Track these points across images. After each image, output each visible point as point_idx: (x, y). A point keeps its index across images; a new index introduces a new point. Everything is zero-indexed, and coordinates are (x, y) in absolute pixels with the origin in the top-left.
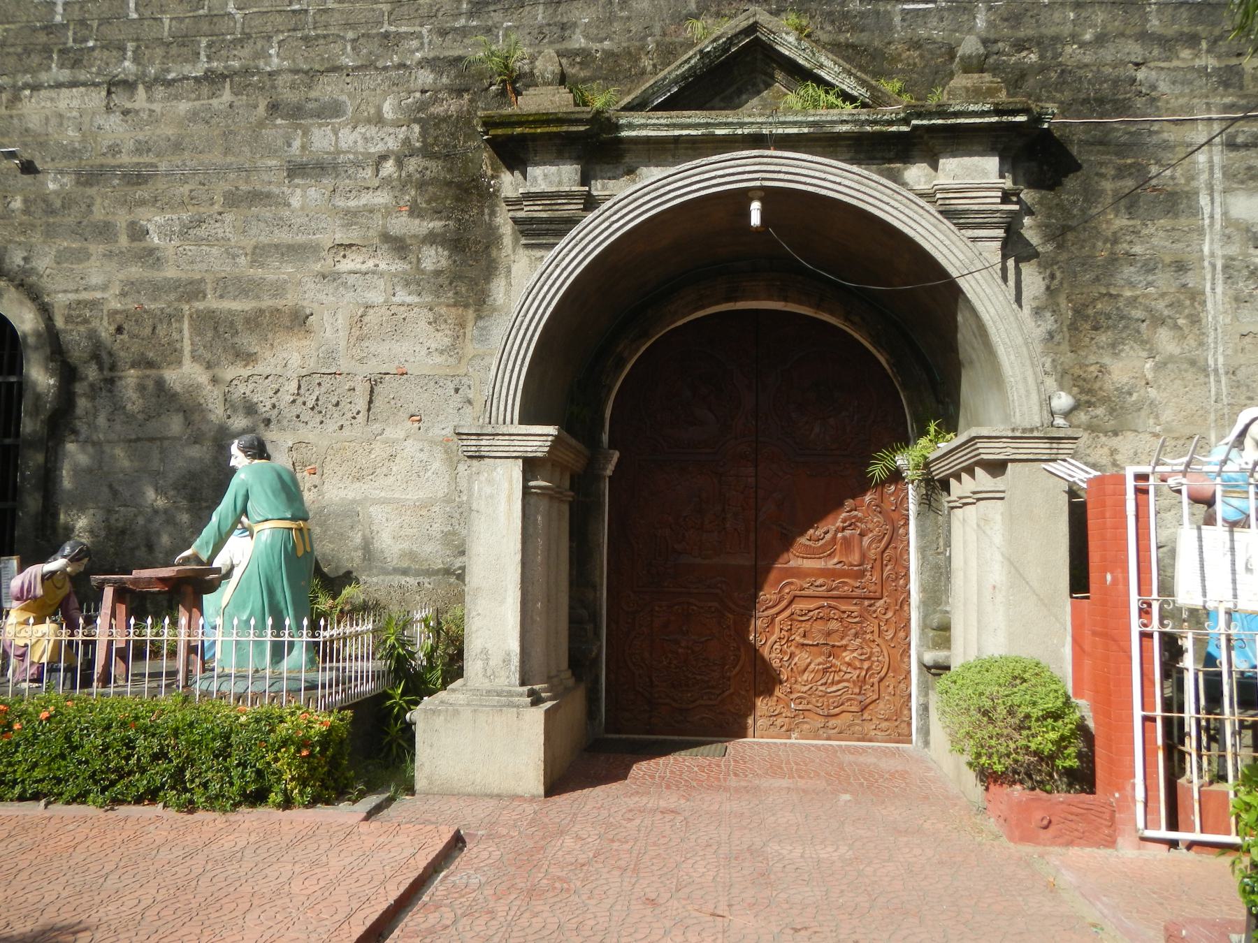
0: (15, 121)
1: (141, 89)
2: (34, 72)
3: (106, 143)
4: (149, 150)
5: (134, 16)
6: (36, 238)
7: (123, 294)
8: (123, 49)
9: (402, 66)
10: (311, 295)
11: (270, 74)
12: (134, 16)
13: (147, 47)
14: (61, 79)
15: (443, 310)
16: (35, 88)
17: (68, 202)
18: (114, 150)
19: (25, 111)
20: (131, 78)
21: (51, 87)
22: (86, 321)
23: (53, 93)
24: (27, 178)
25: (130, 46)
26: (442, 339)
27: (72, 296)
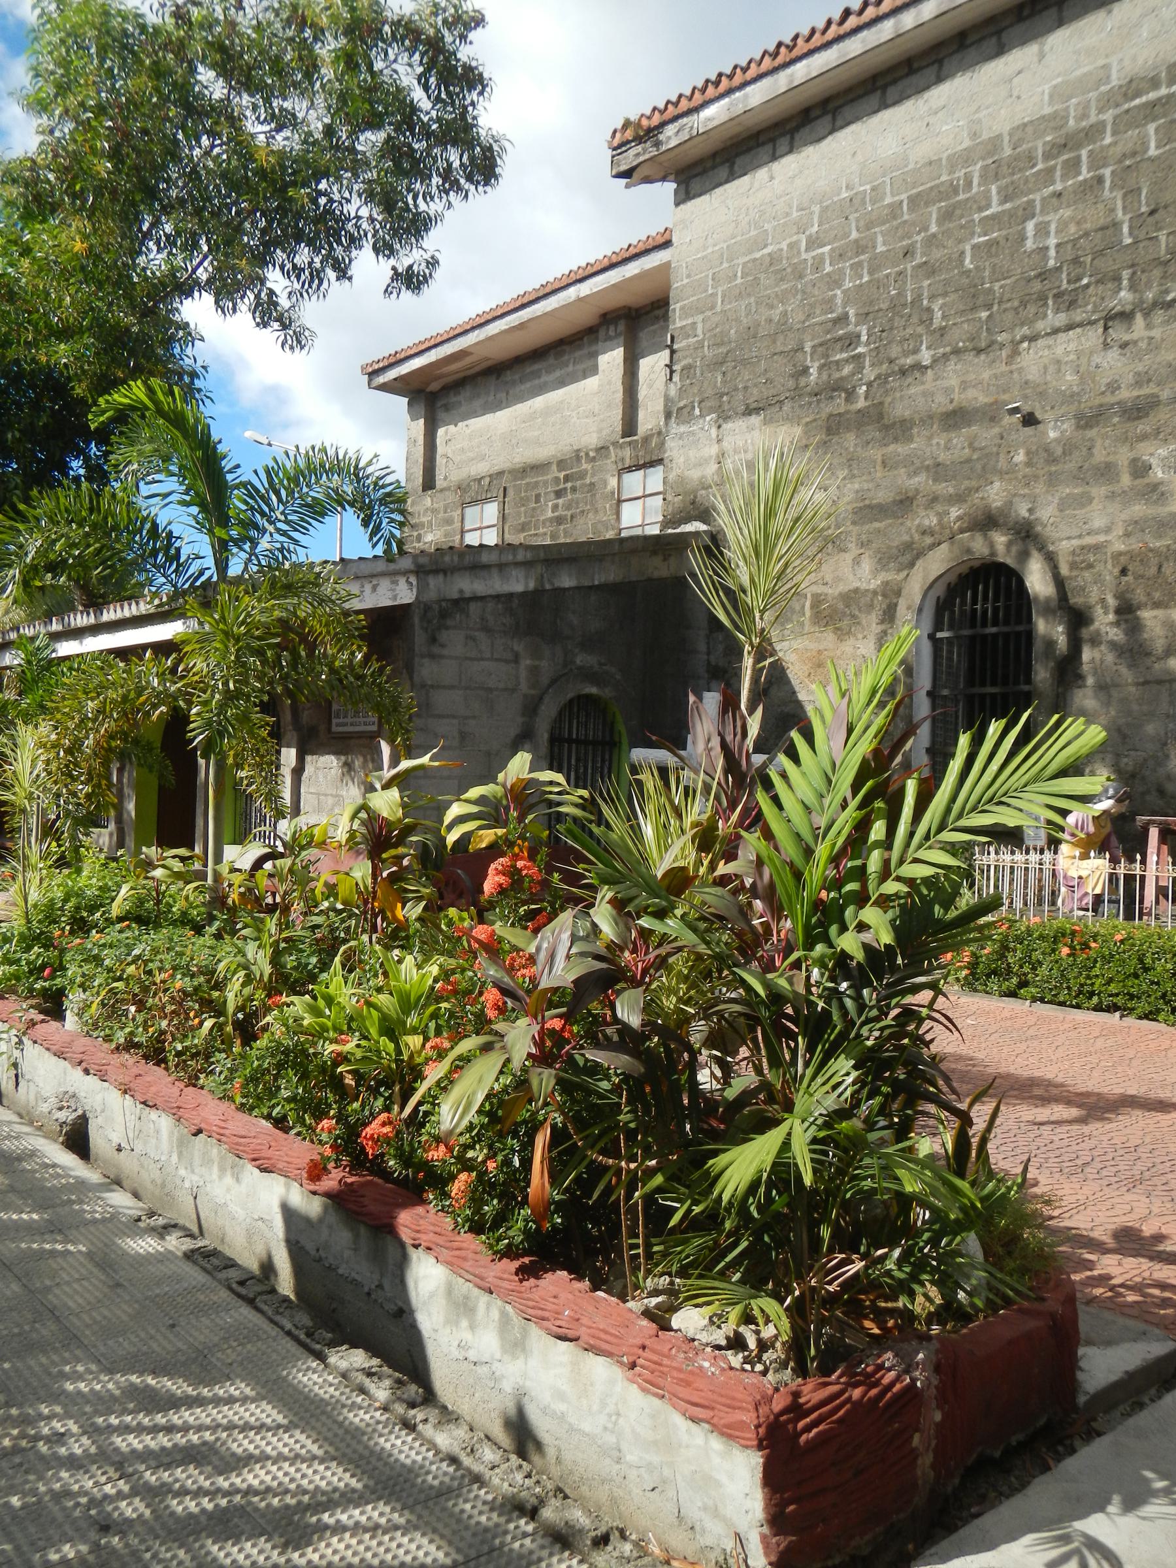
0: (1015, 375)
1: (1139, 317)
2: (1031, 322)
3: (1105, 381)
4: (1149, 381)
5: (1128, 241)
6: (1039, 488)
7: (1127, 535)
8: (1117, 279)
12: (1128, 241)
13: (1143, 271)
14: (1057, 324)
16: (1032, 339)
17: (1069, 447)
18: (1113, 387)
19: (1024, 364)
20: (1128, 308)
21: (1047, 334)
22: (1090, 566)
23: (1050, 341)
24: (1029, 431)
25: (1126, 274)
27: (1076, 542)
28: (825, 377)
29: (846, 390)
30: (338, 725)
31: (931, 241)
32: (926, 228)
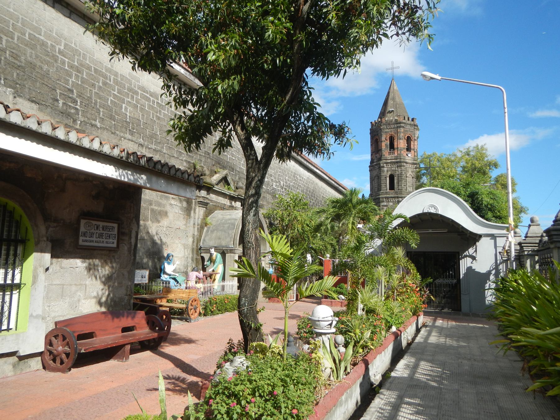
9: (182, 160)
10: (168, 208)
11: (164, 153)
15: (185, 216)
16: (125, 138)
25: (142, 135)
26: (184, 222)
28: (65, 108)
29: (73, 119)
30: (83, 241)
31: (100, 88)
32: (99, 83)
